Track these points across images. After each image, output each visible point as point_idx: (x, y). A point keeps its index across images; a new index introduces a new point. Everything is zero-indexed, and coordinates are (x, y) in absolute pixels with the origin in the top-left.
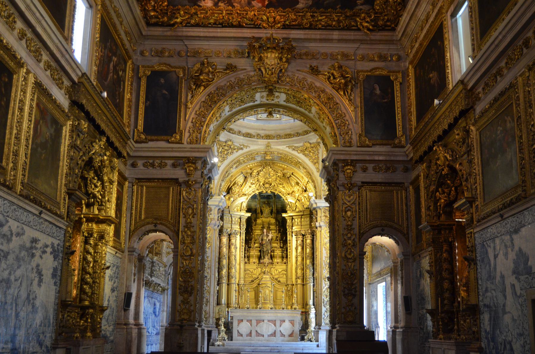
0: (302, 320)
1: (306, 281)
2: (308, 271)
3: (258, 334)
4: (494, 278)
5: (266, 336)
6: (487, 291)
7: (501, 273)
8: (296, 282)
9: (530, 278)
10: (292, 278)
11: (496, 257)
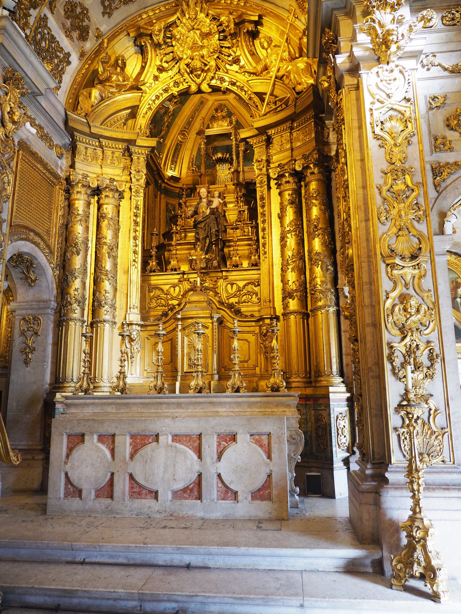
0: (302, 423)
1: (315, 300)
2: (318, 270)
3: (138, 490)
5: (166, 496)
8: (285, 306)
10: (272, 300)
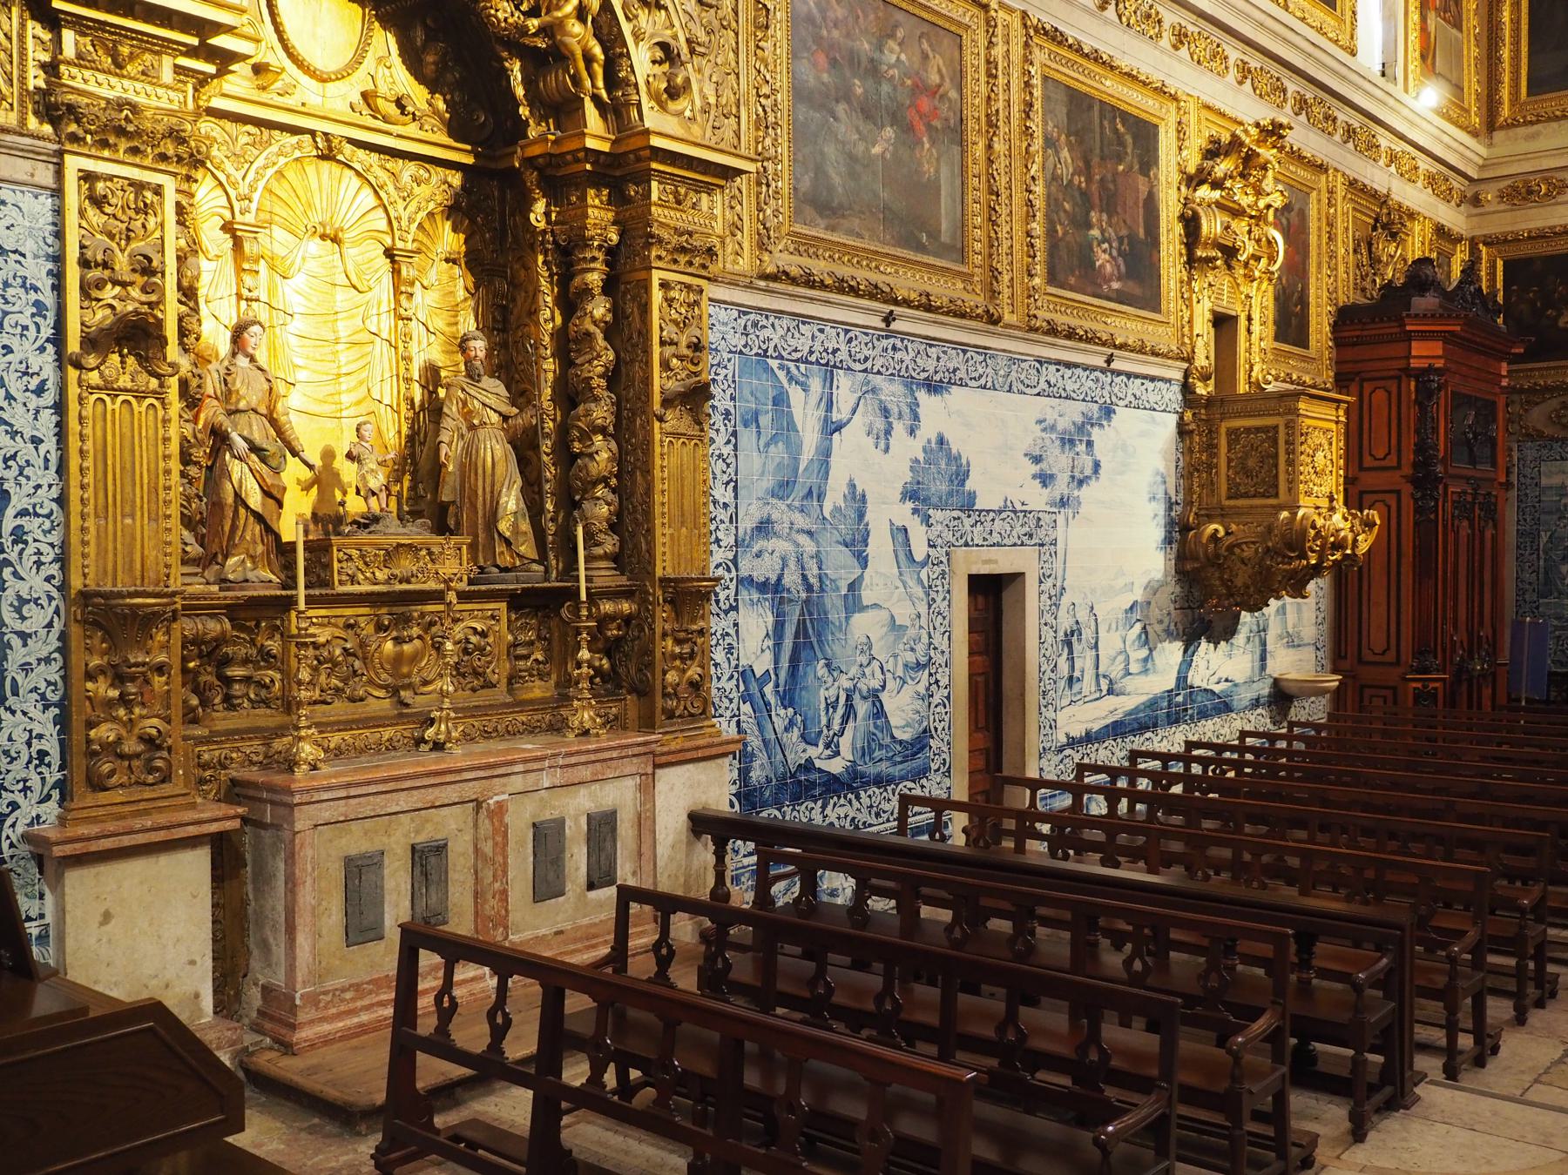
4: (816, 494)
6: (764, 528)
7: (852, 486)
9: (968, 522)
11: (832, 428)
